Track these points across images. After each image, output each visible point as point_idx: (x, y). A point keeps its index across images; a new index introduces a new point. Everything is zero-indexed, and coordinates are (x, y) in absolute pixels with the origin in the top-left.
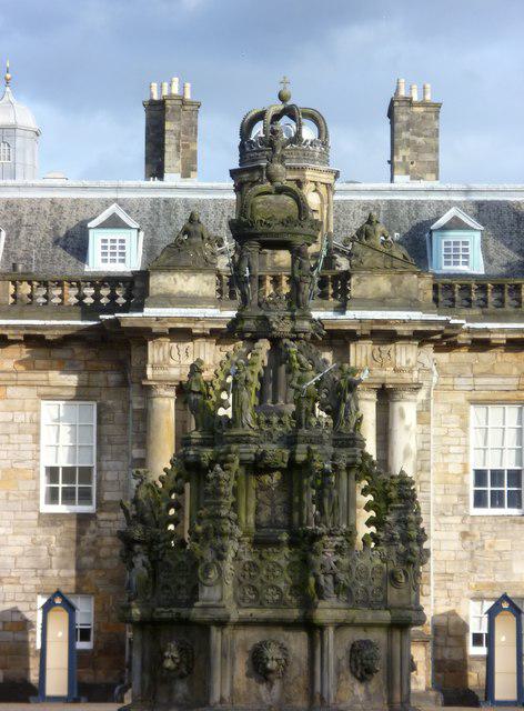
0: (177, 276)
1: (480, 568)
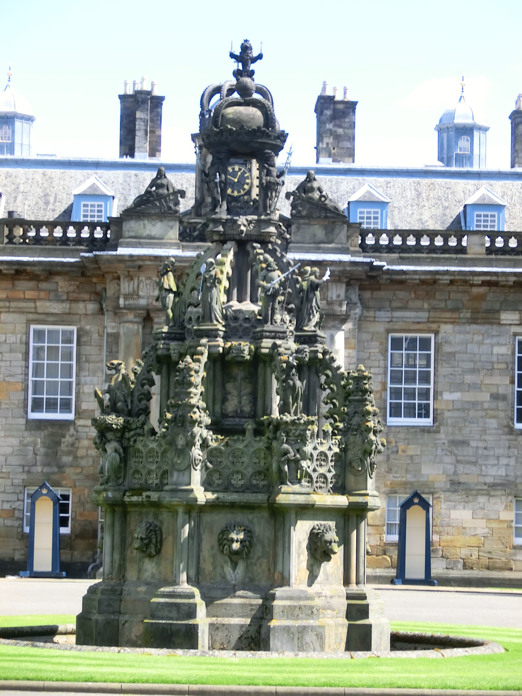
0: (146, 222)
1: (395, 469)
